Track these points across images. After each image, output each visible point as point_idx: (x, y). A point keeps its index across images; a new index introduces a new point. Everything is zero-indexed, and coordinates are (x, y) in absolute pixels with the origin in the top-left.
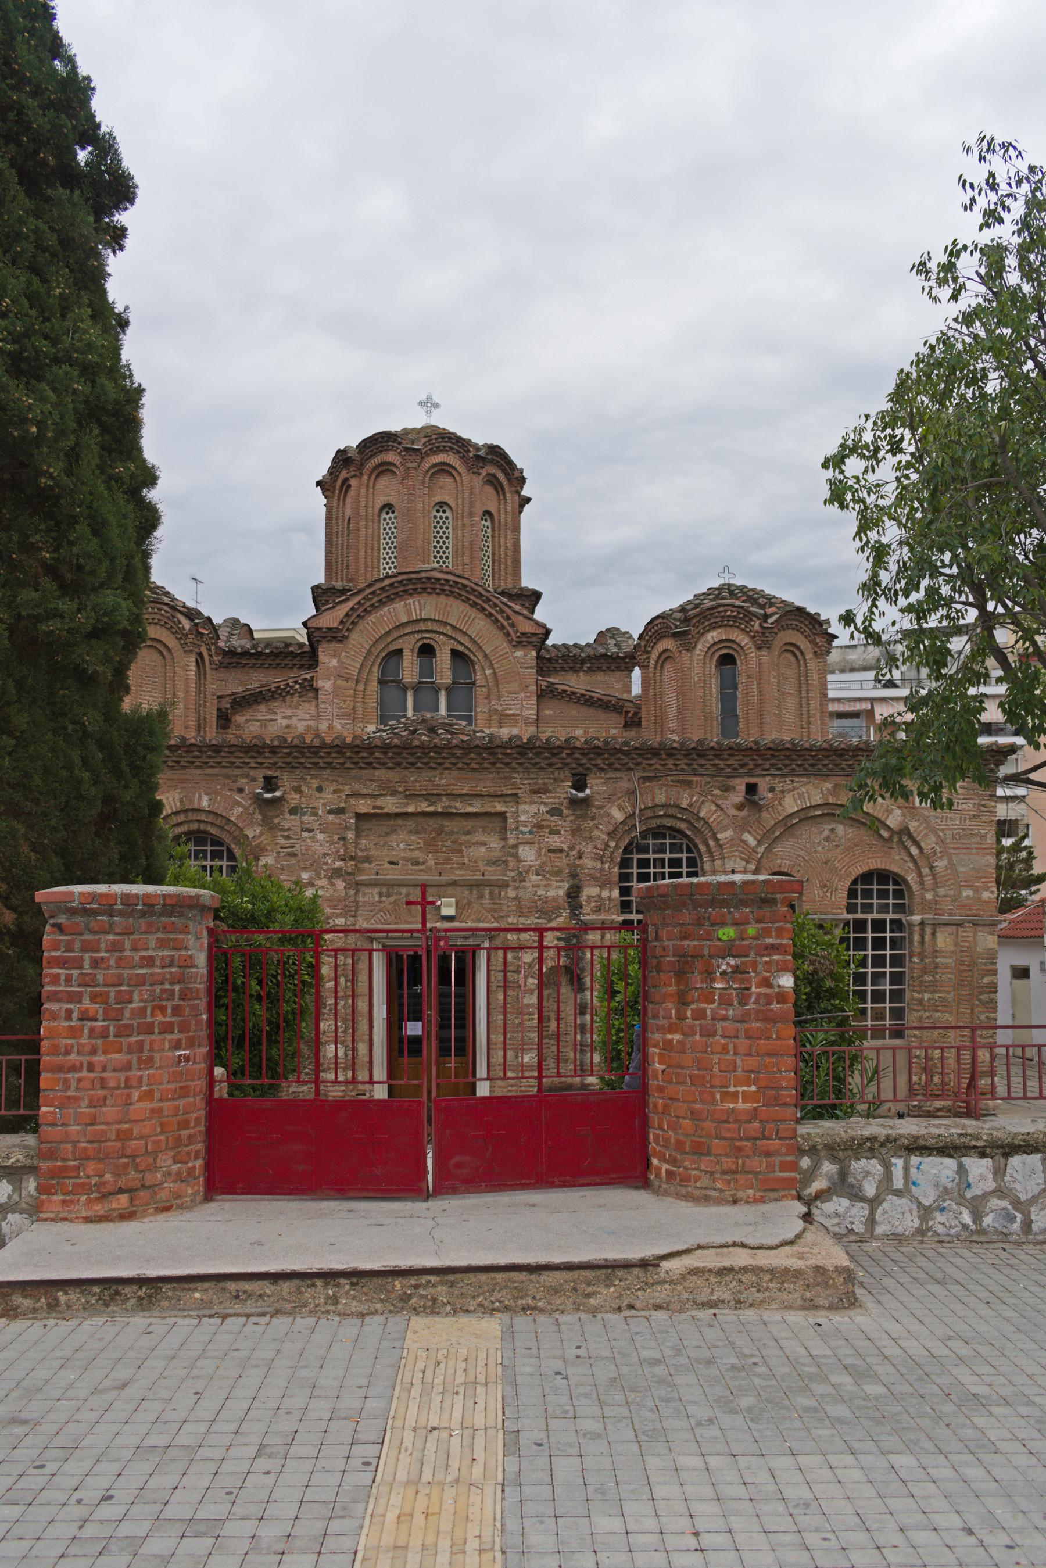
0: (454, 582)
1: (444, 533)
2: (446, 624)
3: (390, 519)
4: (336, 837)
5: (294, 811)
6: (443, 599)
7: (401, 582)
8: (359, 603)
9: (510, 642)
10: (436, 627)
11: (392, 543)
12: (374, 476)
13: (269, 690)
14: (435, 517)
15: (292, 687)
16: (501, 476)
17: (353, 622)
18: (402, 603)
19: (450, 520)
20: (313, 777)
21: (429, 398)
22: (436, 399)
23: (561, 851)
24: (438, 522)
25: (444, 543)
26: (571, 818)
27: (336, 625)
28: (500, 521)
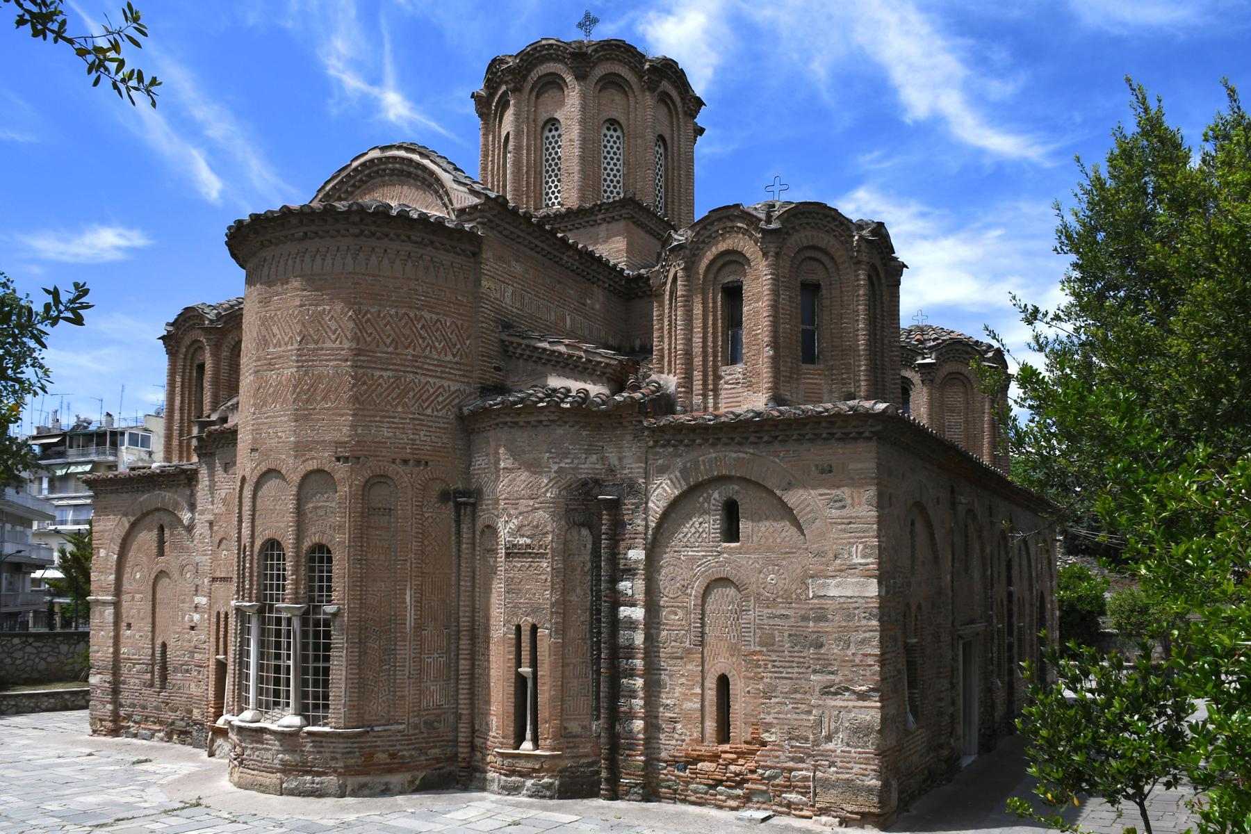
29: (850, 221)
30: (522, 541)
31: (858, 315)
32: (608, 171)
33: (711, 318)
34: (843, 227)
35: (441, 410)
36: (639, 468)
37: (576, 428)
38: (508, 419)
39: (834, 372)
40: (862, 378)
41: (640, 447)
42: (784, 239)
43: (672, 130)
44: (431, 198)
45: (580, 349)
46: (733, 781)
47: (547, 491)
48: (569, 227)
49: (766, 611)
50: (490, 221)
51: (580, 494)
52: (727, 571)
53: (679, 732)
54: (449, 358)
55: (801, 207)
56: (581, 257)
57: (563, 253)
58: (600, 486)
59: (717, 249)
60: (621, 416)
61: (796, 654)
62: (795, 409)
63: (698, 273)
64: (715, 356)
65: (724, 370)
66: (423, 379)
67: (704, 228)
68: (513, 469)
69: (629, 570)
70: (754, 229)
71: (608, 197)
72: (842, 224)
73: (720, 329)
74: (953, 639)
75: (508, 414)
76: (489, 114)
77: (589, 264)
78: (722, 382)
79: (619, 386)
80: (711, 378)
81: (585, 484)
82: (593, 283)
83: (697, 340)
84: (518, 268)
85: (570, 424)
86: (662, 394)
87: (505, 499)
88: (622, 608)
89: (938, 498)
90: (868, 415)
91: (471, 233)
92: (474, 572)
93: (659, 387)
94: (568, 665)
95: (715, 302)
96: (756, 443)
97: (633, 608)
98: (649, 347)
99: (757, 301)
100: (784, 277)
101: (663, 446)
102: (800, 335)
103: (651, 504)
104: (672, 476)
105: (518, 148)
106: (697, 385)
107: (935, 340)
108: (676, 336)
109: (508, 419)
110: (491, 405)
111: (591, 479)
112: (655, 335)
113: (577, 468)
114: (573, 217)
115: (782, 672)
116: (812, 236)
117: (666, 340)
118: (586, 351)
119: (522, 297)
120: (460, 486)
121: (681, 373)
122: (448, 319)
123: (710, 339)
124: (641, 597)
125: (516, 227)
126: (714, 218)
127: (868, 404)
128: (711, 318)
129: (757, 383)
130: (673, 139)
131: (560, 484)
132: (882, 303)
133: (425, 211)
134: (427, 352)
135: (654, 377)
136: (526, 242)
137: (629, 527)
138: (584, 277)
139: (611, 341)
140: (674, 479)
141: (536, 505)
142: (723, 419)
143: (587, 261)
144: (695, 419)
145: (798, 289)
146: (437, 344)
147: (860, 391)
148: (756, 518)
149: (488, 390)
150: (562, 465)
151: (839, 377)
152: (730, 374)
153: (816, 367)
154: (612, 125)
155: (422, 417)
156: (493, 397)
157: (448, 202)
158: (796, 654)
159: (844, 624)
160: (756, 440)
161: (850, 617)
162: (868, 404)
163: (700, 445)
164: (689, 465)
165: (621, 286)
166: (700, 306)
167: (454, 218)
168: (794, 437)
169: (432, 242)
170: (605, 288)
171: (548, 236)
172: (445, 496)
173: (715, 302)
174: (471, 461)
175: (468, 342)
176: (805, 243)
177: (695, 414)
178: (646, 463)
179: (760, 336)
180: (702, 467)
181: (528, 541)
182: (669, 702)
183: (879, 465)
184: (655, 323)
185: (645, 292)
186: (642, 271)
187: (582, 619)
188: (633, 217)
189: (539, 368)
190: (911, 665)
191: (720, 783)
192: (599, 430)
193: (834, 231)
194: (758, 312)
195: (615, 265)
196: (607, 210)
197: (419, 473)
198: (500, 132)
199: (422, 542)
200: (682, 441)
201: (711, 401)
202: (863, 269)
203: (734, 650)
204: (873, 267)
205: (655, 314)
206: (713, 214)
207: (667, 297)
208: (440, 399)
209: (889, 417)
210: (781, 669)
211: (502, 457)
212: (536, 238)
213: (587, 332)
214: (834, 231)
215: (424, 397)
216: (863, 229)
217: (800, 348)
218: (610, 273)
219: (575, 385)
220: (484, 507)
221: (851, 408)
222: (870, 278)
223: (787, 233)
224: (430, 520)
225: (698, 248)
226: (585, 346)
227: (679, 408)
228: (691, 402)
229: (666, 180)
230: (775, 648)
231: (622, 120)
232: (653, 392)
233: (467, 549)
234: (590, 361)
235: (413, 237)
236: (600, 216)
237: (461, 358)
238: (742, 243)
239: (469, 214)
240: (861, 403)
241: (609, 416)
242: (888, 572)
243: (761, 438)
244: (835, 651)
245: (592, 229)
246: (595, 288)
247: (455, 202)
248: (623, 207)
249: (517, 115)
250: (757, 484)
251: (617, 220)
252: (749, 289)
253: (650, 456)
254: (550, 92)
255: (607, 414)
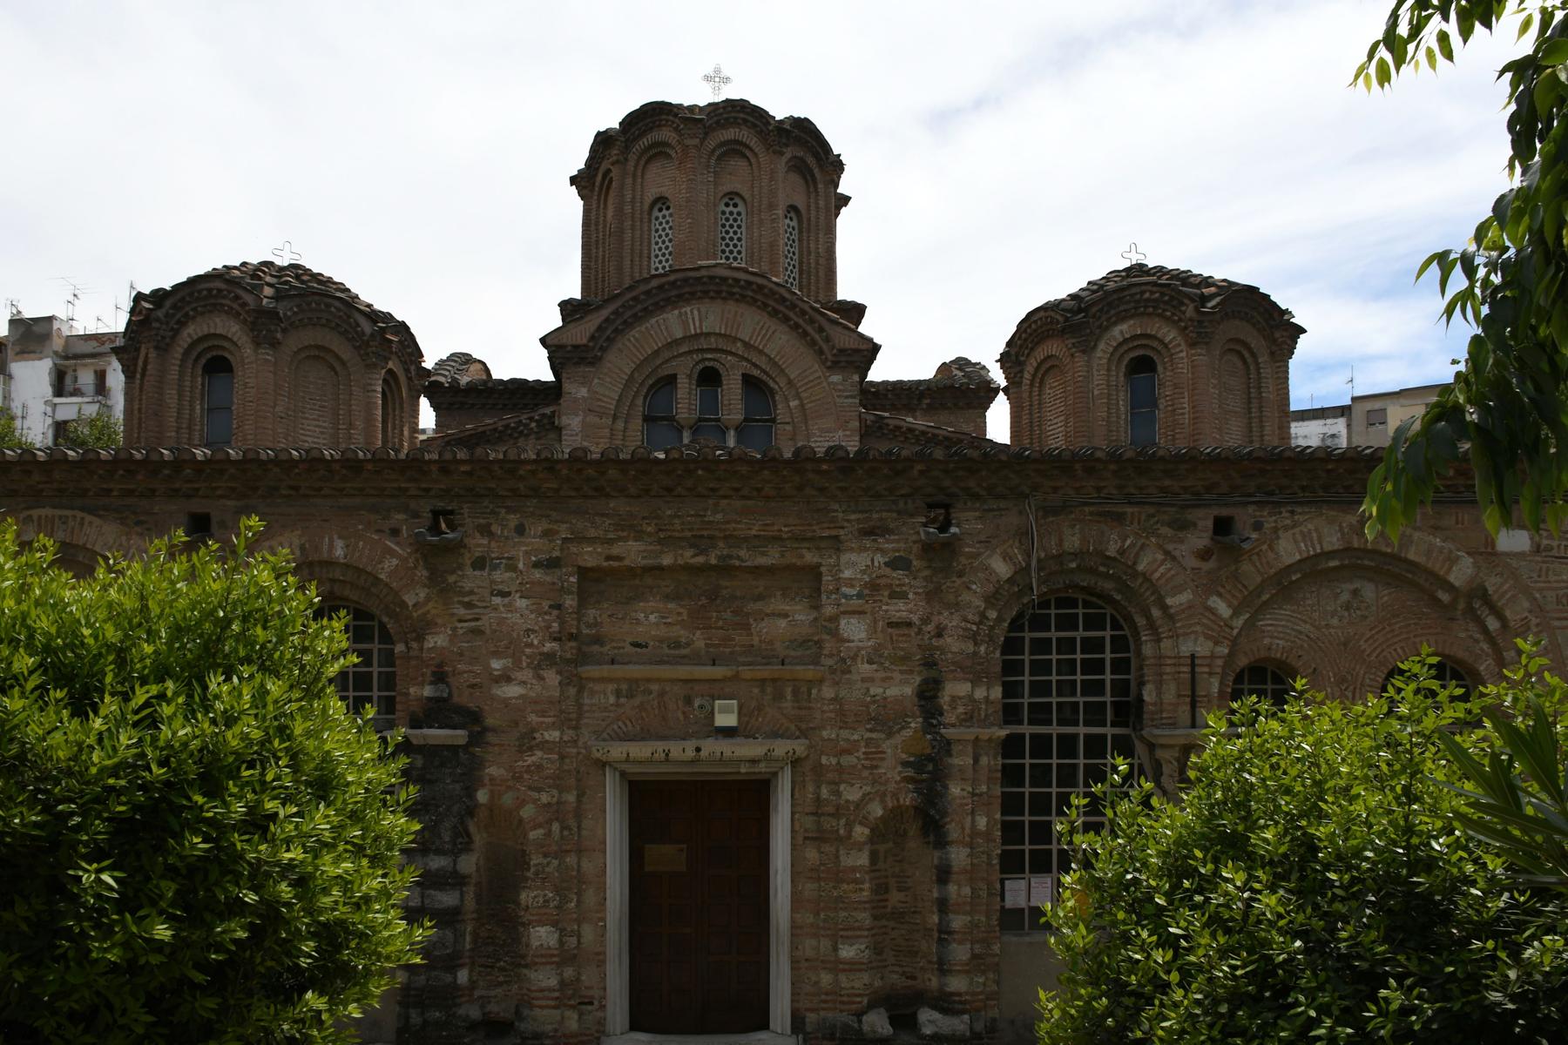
0: (746, 281)
1: (735, 233)
2: (735, 339)
3: (664, 217)
4: (546, 605)
5: (479, 564)
6: (731, 307)
7: (673, 283)
8: (616, 313)
9: (824, 362)
10: (722, 344)
11: (667, 248)
12: (642, 162)
13: (495, 429)
14: (723, 213)
15: (526, 425)
16: (810, 160)
17: (608, 339)
18: (676, 312)
19: (743, 216)
20: (510, 510)
21: (718, 71)
22: (725, 72)
23: (909, 624)
24: (727, 220)
25: (735, 246)
26: (926, 573)
27: (585, 341)
28: (809, 219)
154: (731, 199)
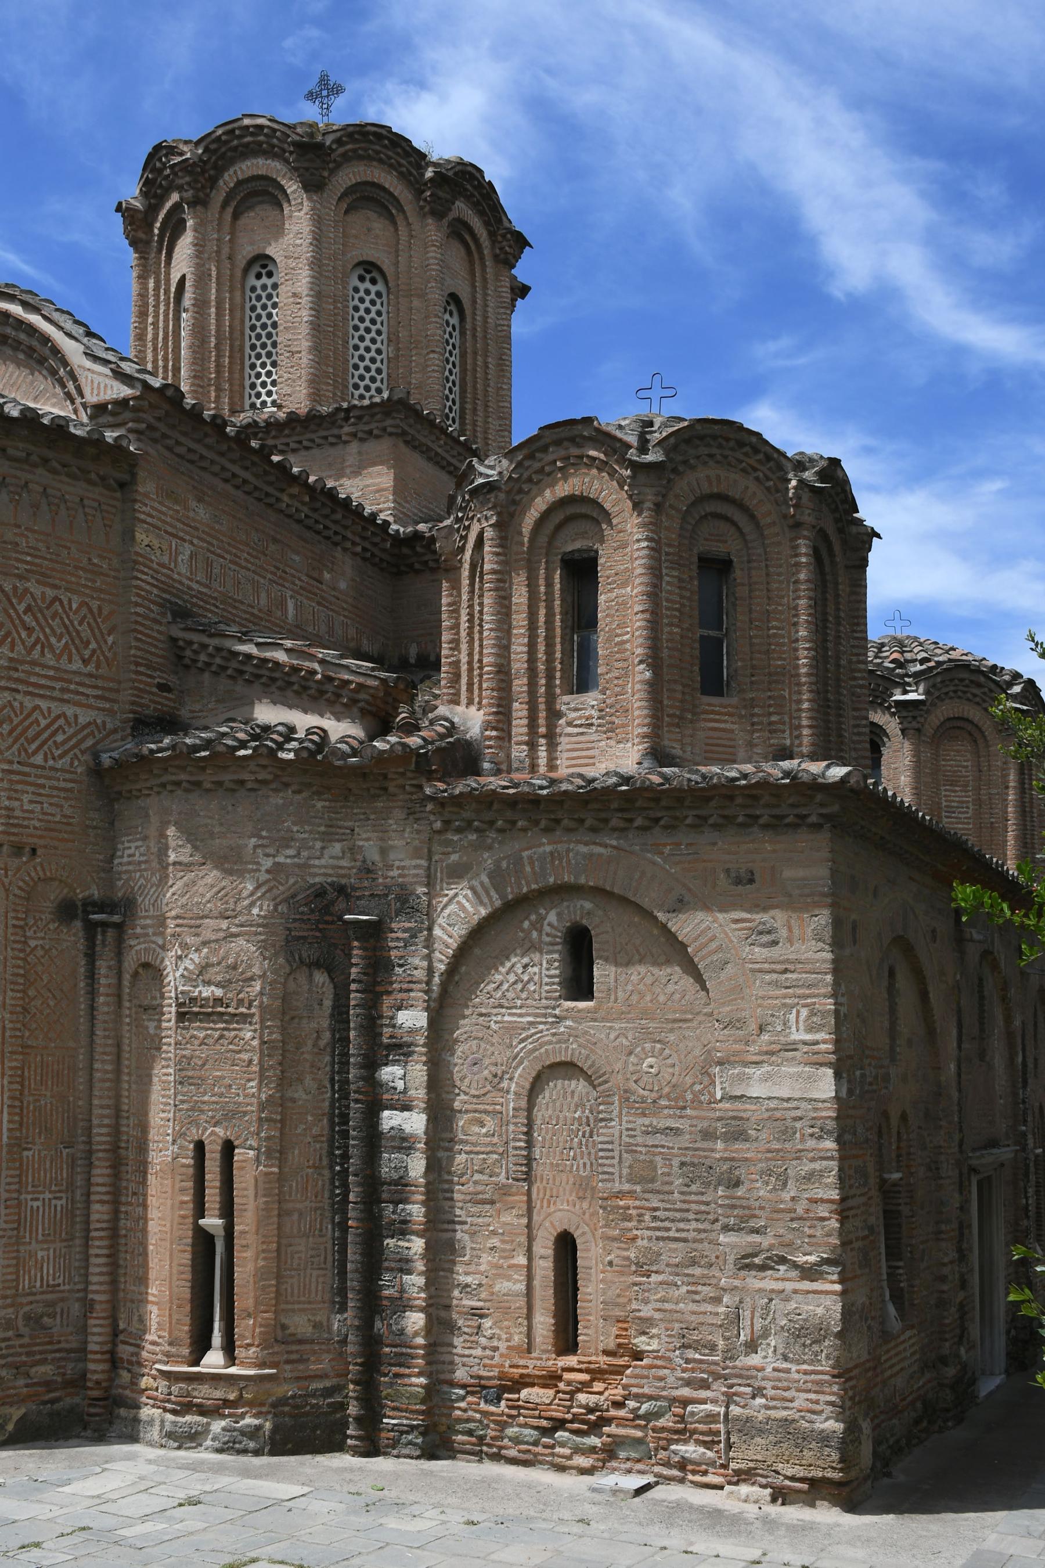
29: (783, 454)
30: (207, 992)
31: (797, 616)
32: (362, 351)
33: (542, 612)
34: (772, 464)
35: (61, 757)
36: (416, 867)
37: (305, 794)
38: (183, 777)
39: (756, 710)
40: (805, 722)
41: (418, 832)
42: (669, 481)
43: (474, 287)
44: (43, 382)
45: (312, 657)
46: (583, 1422)
47: (252, 904)
48: (293, 445)
49: (640, 1121)
50: (150, 427)
51: (312, 911)
52: (572, 1051)
53: (488, 1333)
54: (77, 665)
55: (698, 427)
56: (313, 498)
57: (282, 490)
58: (348, 896)
59: (553, 493)
60: (385, 777)
61: (693, 1198)
62: (689, 772)
63: (520, 533)
64: (550, 677)
65: (566, 702)
66: (29, 703)
67: (531, 456)
68: (191, 864)
69: (399, 1046)
70: (617, 462)
71: (362, 397)
72: (768, 458)
73: (558, 631)
74: (961, 1174)
75: (183, 768)
76: (148, 242)
77: (327, 511)
78: (562, 722)
79: (382, 726)
80: (542, 714)
81: (320, 893)
82: (336, 544)
83: (519, 648)
84: (202, 513)
85: (295, 787)
86: (458, 740)
87: (177, 917)
88: (386, 1113)
89: (934, 931)
90: (816, 787)
91: (118, 449)
92: (119, 1046)
93: (452, 728)
94: (289, 1213)
95: (549, 585)
96: (623, 830)
97: (406, 1114)
98: (432, 658)
99: (624, 585)
100: (669, 545)
101: (459, 830)
102: (697, 645)
103: (437, 932)
104: (475, 883)
105: (201, 304)
106: (519, 727)
107: (923, 661)
108: (481, 640)
109: (183, 777)
110: (152, 751)
111: (332, 884)
112: (445, 637)
113: (305, 866)
114: (298, 429)
115: (668, 1229)
116: (718, 477)
117: (464, 647)
118: (322, 662)
119: (209, 564)
120: (95, 893)
121: (491, 705)
122: (75, 597)
123: (541, 648)
124: (419, 1093)
125: (199, 441)
126: (548, 440)
127: (815, 767)
128: (542, 612)
129: (623, 726)
130: (474, 302)
131: (275, 892)
132: (837, 596)
133: (32, 405)
134: (36, 653)
135: (443, 710)
136: (216, 468)
137: (398, 970)
138: (318, 533)
139: (366, 646)
140: (479, 889)
141: (234, 930)
142: (564, 787)
143: (323, 504)
144: (516, 785)
145: (694, 567)
146: (53, 640)
147: (800, 745)
148: (624, 959)
149: (147, 725)
150: (280, 859)
151: (765, 720)
152: (576, 710)
153: (724, 700)
154: (368, 272)
155: (27, 769)
156: (156, 737)
157: (73, 392)
158: (693, 1198)
159: (776, 1146)
160: (622, 824)
161: (786, 1133)
162: (815, 767)
163: (524, 830)
164: (504, 864)
165: (384, 550)
166: (524, 590)
167: (85, 419)
168: (689, 821)
169: (46, 461)
170: (355, 554)
171: (256, 459)
172: (67, 911)
173: (549, 585)
174: (115, 850)
175: (110, 640)
176: (706, 489)
177: (516, 776)
178: (430, 859)
179: (628, 646)
180: (528, 869)
181: (219, 992)
182: (469, 1279)
183: (834, 873)
184: (444, 616)
185: (426, 562)
186: (422, 527)
187: (315, 1131)
188: (404, 433)
189: (239, 688)
190: (891, 1216)
191: (560, 1424)
192: (346, 799)
193: (755, 470)
194: (624, 603)
195: (374, 515)
196: (359, 418)
197: (19, 869)
198: (168, 274)
199: (24, 991)
200: (492, 823)
201: (542, 754)
202: (805, 538)
203: (584, 1188)
204: (822, 534)
205: (444, 601)
206: (547, 433)
207: (465, 573)
208: (60, 738)
209: (852, 790)
210: (667, 1224)
211: (172, 843)
212: (233, 462)
213: (323, 628)
214: (755, 470)
215: (30, 733)
216: (805, 469)
217: (696, 668)
218: (364, 528)
219: (303, 721)
220: (138, 930)
221: (787, 774)
222: (816, 554)
223: (674, 470)
224: (40, 952)
225: (520, 491)
226: (321, 653)
227: (486, 765)
228: (509, 756)
229: (464, 371)
230: (657, 1186)
231: (386, 265)
232: (442, 737)
233: (107, 1004)
234: (330, 679)
235: (10, 451)
236: (347, 429)
237: (98, 667)
238: (596, 485)
239: (113, 414)
240: (804, 766)
241: (364, 775)
242: (850, 1057)
243: (631, 821)
244: (762, 1193)
245: (332, 451)
246: (338, 553)
247: (87, 391)
248: (387, 414)
249: (199, 246)
250: (624, 900)
251: (377, 437)
252: (608, 565)
253: (436, 848)
254: (257, 209)
255: (361, 773)
